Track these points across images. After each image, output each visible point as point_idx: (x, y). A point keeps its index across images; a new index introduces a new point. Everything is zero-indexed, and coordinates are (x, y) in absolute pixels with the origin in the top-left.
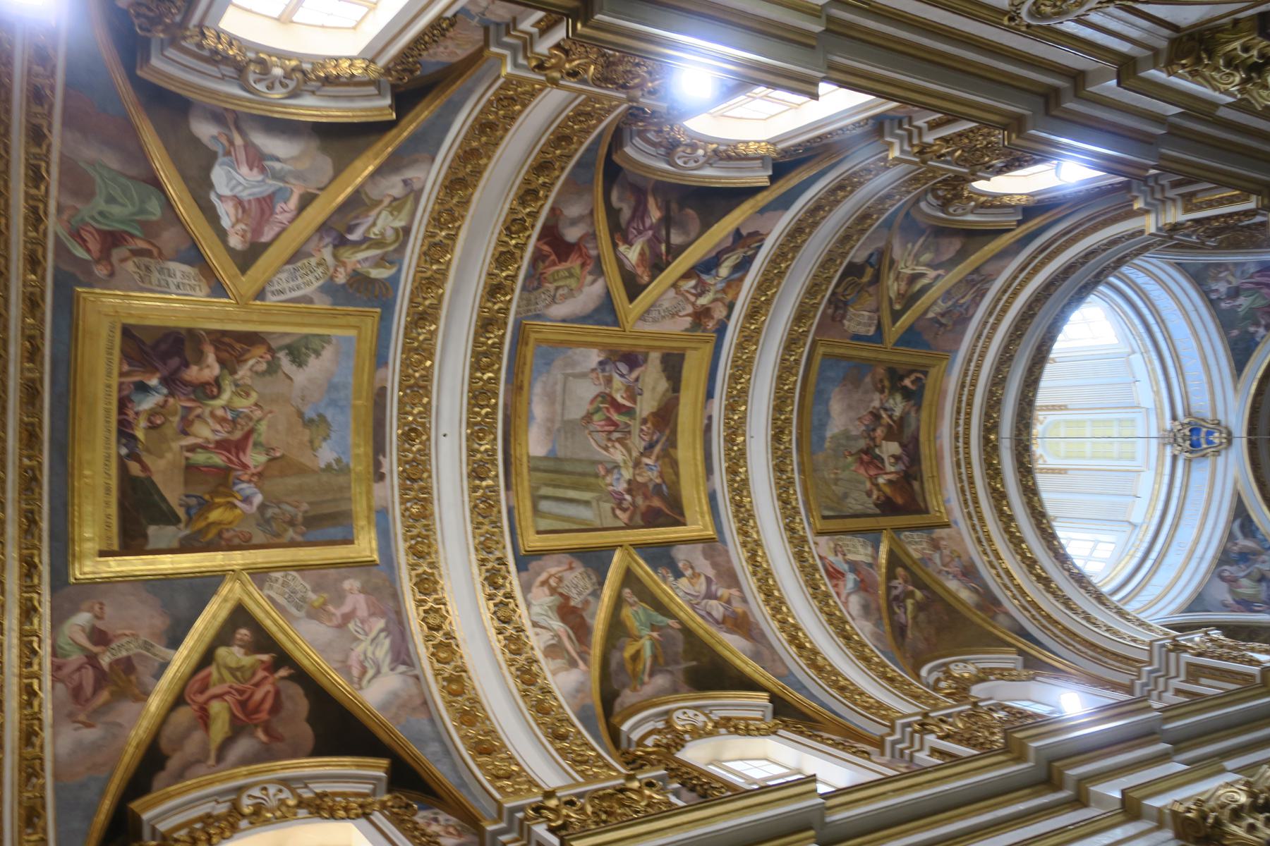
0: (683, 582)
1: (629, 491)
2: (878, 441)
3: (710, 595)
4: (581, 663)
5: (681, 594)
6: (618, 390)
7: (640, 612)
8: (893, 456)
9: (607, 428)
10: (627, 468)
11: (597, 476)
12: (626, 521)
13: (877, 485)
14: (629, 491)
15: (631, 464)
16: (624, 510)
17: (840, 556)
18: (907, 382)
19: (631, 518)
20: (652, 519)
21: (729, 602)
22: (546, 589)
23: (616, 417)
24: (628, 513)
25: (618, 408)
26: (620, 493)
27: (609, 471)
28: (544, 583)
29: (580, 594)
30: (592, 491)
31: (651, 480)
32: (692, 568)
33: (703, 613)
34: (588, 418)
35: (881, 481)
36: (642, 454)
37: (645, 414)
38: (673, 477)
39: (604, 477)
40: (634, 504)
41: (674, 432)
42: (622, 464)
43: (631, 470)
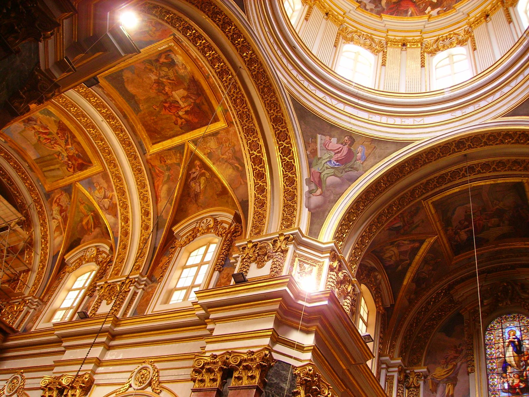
0: (96, 192)
1: (69, 160)
2: (169, 93)
3: (105, 197)
4: (63, 232)
5: (96, 198)
6: (39, 128)
7: (86, 206)
8: (183, 97)
9: (48, 141)
10: (63, 152)
11: (56, 159)
12: (73, 172)
13: (180, 117)
14: (69, 160)
15: (64, 150)
16: (71, 168)
17: (163, 163)
18: (162, 60)
19: (74, 170)
20: (82, 167)
21: (111, 199)
22: (56, 204)
23: (47, 137)
24: (72, 168)
25: (45, 133)
26: (66, 162)
27: (59, 156)
28: (55, 203)
29: (65, 204)
30: (57, 164)
31: (74, 153)
32: (99, 185)
33: (101, 206)
34: (39, 140)
35: (181, 113)
36: (66, 145)
37: (56, 131)
38: (81, 149)
39: (58, 158)
40: (72, 164)
41: (71, 132)
42: (61, 151)
43: (65, 152)
